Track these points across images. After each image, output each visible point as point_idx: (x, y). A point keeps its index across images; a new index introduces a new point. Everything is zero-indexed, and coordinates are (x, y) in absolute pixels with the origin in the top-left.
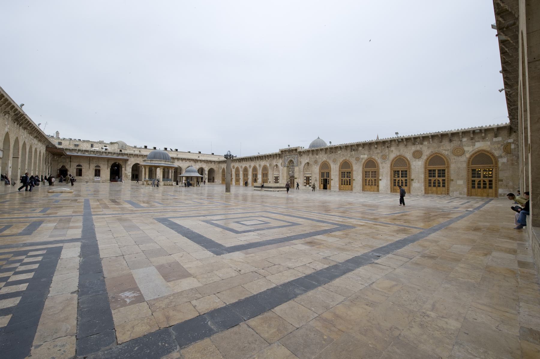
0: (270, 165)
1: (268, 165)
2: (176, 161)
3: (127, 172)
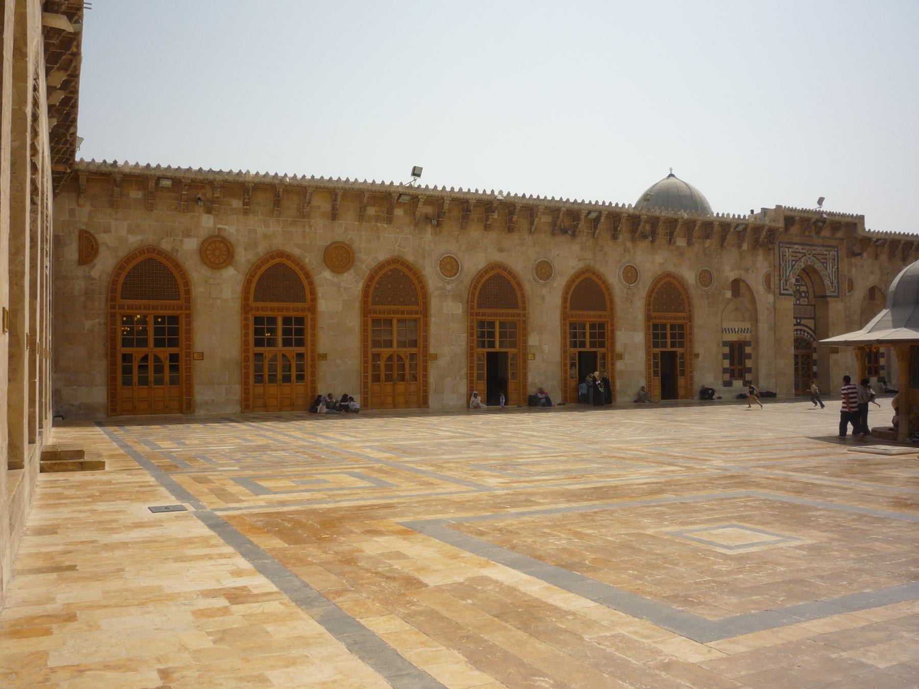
0: (705, 278)
1: (689, 276)
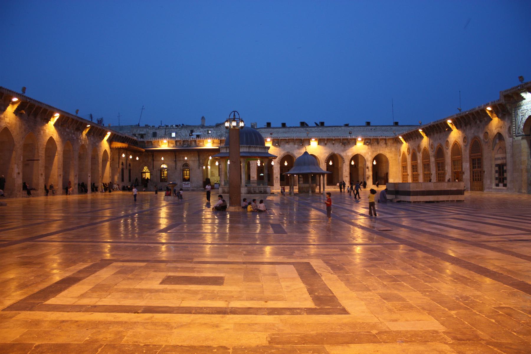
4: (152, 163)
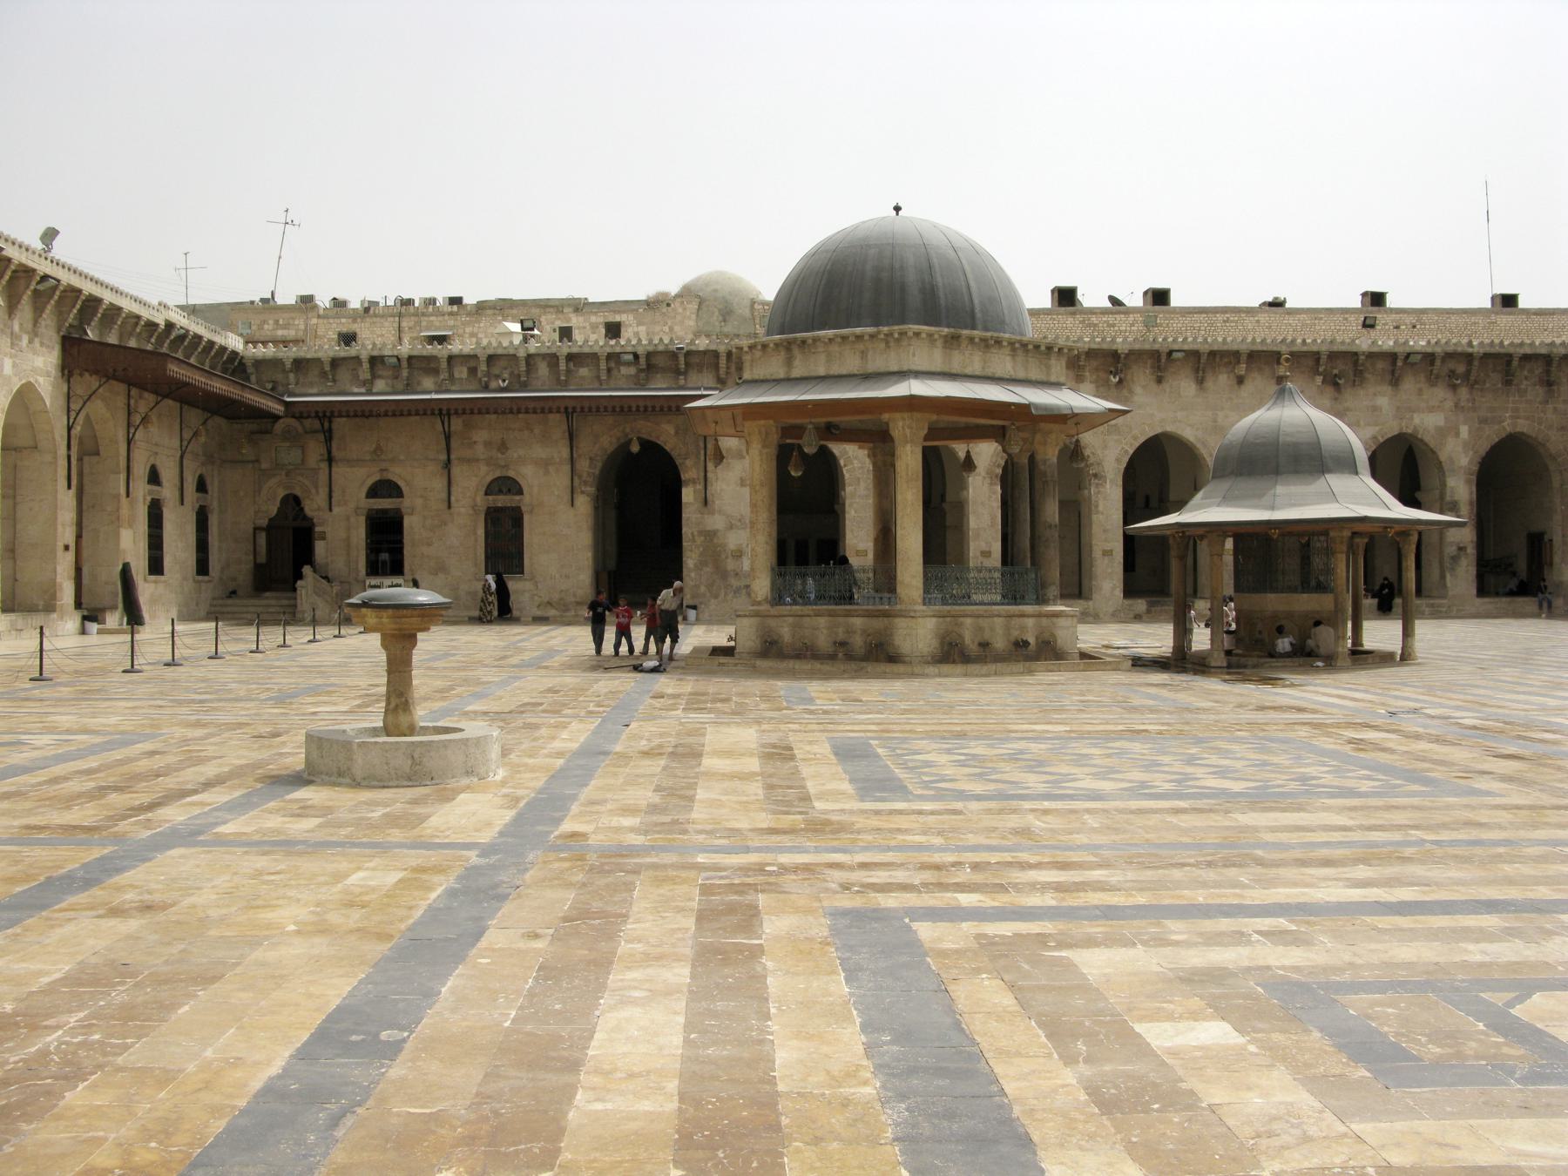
2: (1141, 378)
3: (716, 522)
4: (323, 477)
